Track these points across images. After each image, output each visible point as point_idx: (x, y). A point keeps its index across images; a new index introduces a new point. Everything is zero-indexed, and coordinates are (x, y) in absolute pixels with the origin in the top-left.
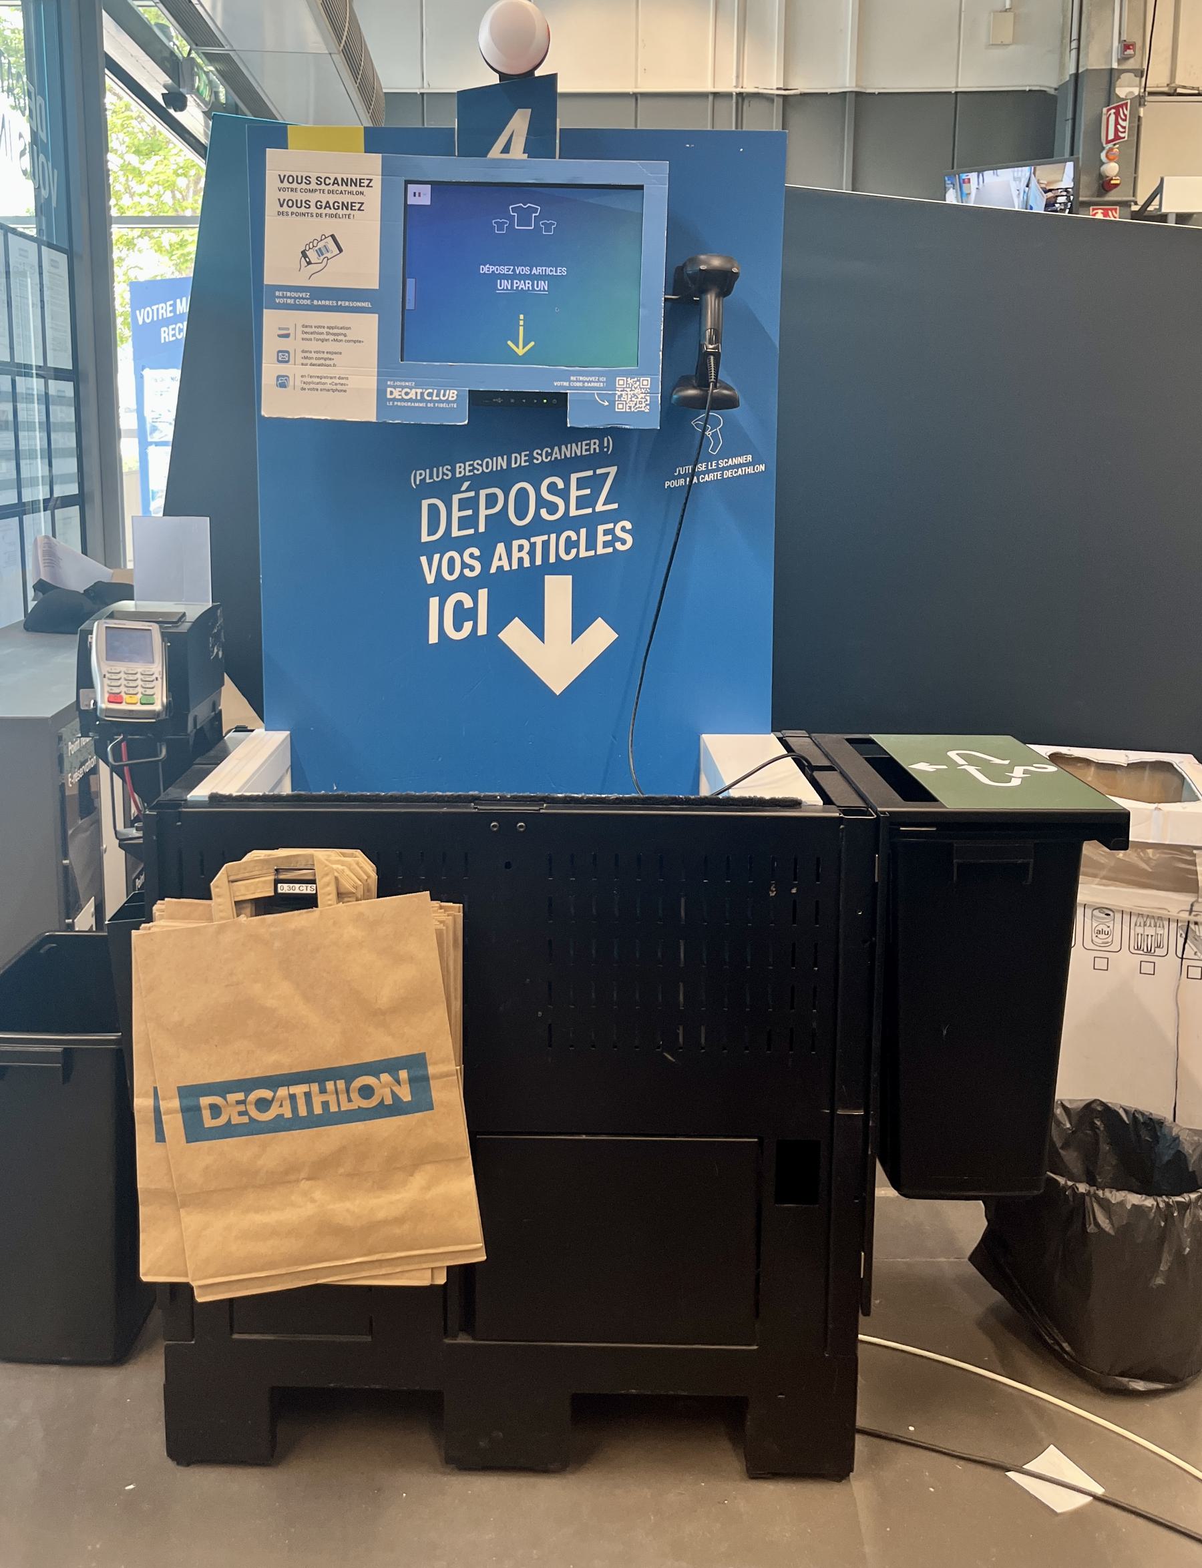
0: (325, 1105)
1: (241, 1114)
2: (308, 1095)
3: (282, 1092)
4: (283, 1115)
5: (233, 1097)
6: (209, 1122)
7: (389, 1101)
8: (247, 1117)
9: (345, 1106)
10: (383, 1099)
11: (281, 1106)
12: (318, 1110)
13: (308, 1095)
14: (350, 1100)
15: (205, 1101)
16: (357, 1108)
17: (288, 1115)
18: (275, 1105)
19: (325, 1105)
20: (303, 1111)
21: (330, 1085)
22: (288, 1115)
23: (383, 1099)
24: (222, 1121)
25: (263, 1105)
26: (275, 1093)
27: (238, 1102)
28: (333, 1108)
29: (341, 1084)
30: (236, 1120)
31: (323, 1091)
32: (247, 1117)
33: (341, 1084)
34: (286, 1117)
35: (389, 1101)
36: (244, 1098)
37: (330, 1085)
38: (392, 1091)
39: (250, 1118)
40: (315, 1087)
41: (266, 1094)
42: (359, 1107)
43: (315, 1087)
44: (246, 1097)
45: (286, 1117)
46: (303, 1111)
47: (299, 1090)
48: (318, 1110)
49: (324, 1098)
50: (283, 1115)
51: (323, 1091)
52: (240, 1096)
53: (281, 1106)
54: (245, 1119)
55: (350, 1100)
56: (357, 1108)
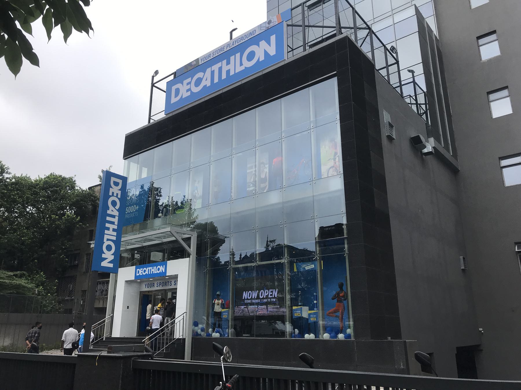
0: (108, 229)
1: (113, 193)
2: (113, 223)
3: (116, 213)
5: (119, 193)
6: (113, 179)
7: (103, 256)
9: (106, 237)
11: (112, 211)
12: (107, 225)
13: (113, 223)
14: (108, 240)
15: (120, 181)
17: (109, 212)
18: (114, 209)
19: (108, 229)
20: (108, 218)
22: (109, 212)
25: (114, 203)
27: (117, 194)
28: (106, 232)
29: (114, 238)
30: (111, 190)
31: (114, 230)
33: (114, 238)
35: (103, 256)
37: (115, 234)
39: (111, 196)
41: (118, 207)
43: (116, 227)
44: (118, 198)
46: (108, 218)
47: (116, 220)
48: (107, 225)
49: (111, 229)
50: (109, 210)
51: (114, 230)
52: (119, 196)
53: (112, 211)
54: (111, 194)
55: (108, 240)
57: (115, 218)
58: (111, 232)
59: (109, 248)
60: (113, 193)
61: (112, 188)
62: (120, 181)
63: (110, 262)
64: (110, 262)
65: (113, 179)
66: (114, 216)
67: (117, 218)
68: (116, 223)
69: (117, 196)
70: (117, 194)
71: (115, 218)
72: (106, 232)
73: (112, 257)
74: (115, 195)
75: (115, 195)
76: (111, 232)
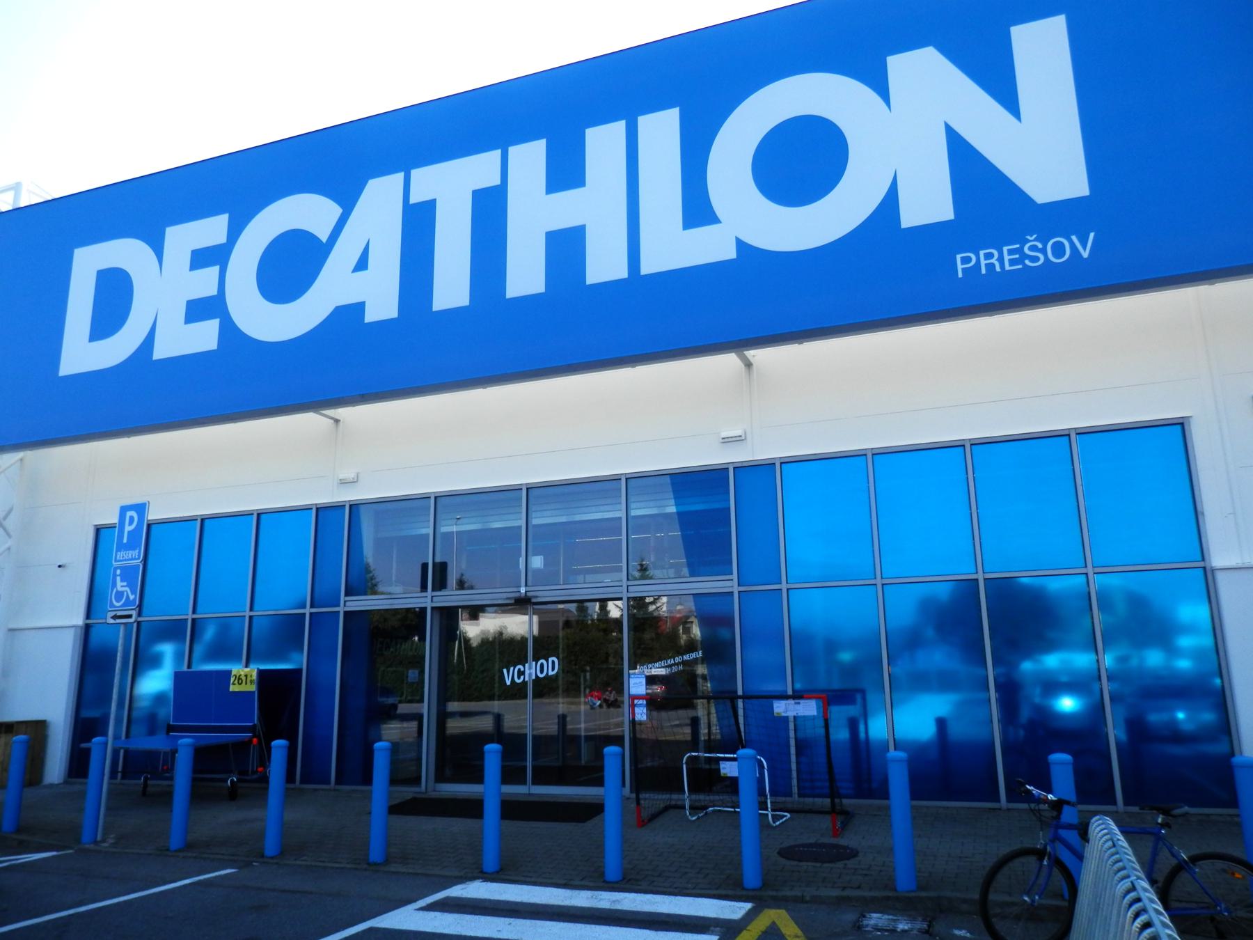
1: (197, 310)
4: (360, 307)
10: (892, 196)
11: (362, 264)
23: (892, 196)
26: (347, 201)
27: (201, 258)
34: (370, 316)
36: (221, 238)
38: (960, 152)
42: (740, 244)
44: (235, 232)
45: (370, 316)
50: (360, 307)
52: (212, 230)
53: (362, 264)
54: (205, 336)
57: (429, 207)
60: (197, 310)
70: (201, 258)
71: (430, 206)
74: (204, 283)
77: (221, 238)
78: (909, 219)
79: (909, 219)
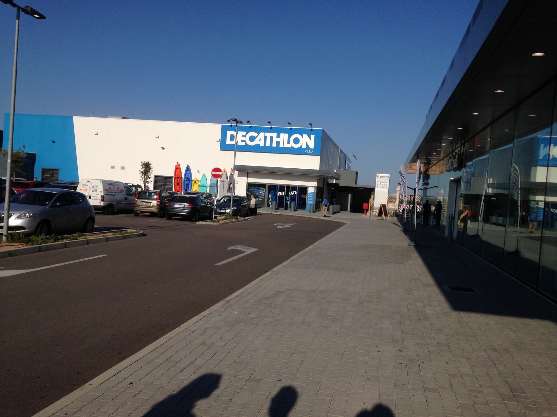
0: (278, 143)
1: (242, 141)
2: (272, 137)
3: (262, 135)
4: (260, 144)
5: (241, 133)
6: (228, 142)
7: (304, 147)
8: (245, 142)
9: (287, 146)
10: (302, 145)
11: (260, 140)
12: (274, 145)
13: (272, 137)
14: (289, 143)
16: (291, 147)
19: (278, 143)
20: (268, 144)
21: (282, 135)
24: (233, 142)
25: (252, 139)
27: (243, 136)
28: (281, 145)
29: (286, 135)
30: (240, 143)
31: (278, 136)
32: (245, 142)
33: (286, 135)
34: (261, 145)
35: (304, 147)
36: (245, 134)
37: (282, 135)
38: (307, 144)
39: (246, 142)
40: (275, 135)
41: (254, 134)
43: (275, 135)
44: (246, 134)
45: (261, 145)
46: (268, 144)
47: (269, 135)
48: (274, 145)
49: (278, 140)
50: (260, 144)
51: (278, 136)
52: (244, 133)
53: (260, 140)
54: (243, 144)
55: (289, 143)
56: (291, 147)
57: (266, 136)
58: (280, 140)
59: (296, 141)
60: (242, 141)
61: (237, 143)
62: (229, 133)
63: (310, 138)
64: (310, 138)
65: (228, 142)
66: (265, 137)
67: (266, 134)
68: (271, 134)
69: (245, 136)
70: (243, 136)
71: (266, 136)
72: (281, 145)
73: (305, 136)
74: (243, 138)
75: (243, 138)
76: (280, 140)
77: (245, 134)
78: (303, 147)
79: (303, 147)
